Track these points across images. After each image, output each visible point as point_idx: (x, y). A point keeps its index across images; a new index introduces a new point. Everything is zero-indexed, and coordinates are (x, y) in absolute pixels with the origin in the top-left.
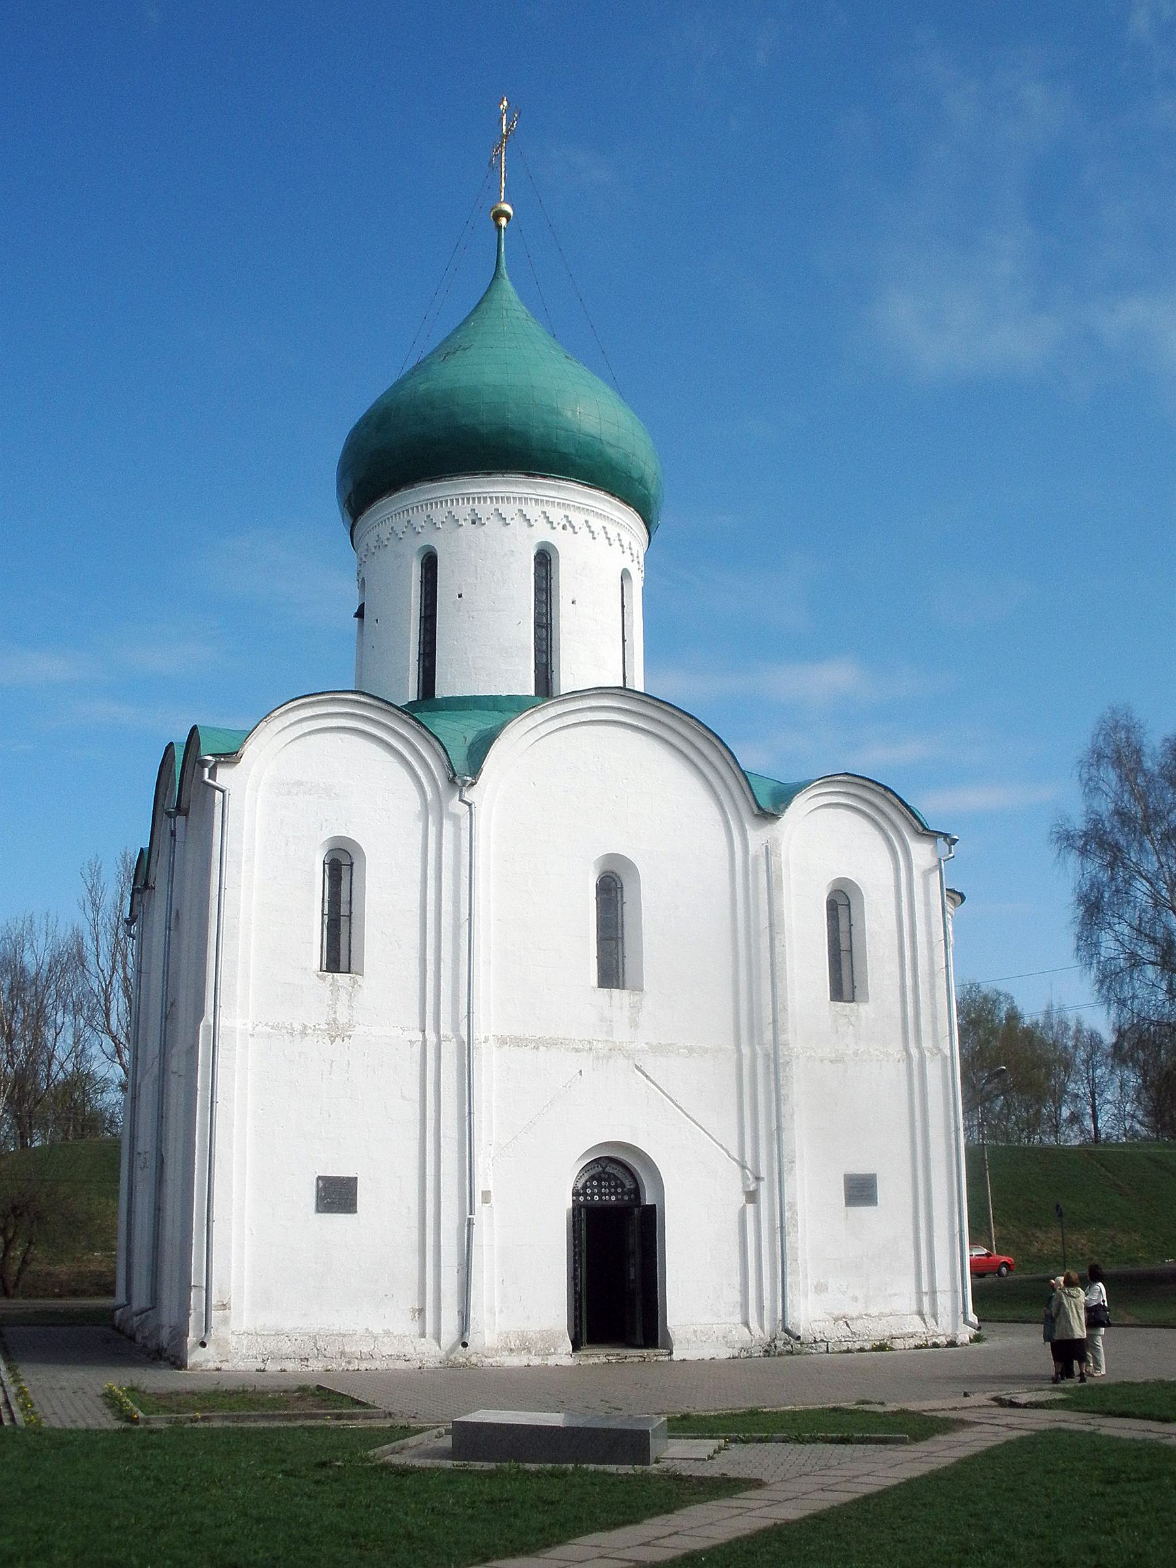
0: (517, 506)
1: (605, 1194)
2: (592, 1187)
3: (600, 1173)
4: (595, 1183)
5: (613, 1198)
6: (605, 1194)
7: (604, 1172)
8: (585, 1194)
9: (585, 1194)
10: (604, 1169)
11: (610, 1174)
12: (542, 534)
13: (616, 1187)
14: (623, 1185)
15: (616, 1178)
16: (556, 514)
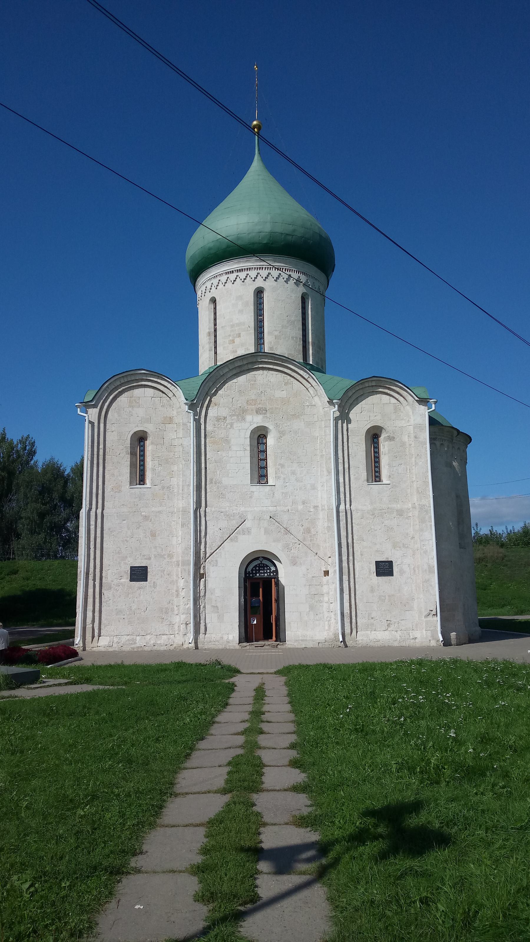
0: (246, 272)
1: (262, 573)
2: (256, 570)
3: (259, 564)
4: (257, 568)
5: (266, 575)
6: (262, 573)
7: (261, 564)
8: (252, 573)
9: (252, 573)
10: (261, 562)
11: (264, 564)
12: (259, 283)
13: (267, 570)
14: (270, 569)
15: (267, 566)
16: (264, 273)
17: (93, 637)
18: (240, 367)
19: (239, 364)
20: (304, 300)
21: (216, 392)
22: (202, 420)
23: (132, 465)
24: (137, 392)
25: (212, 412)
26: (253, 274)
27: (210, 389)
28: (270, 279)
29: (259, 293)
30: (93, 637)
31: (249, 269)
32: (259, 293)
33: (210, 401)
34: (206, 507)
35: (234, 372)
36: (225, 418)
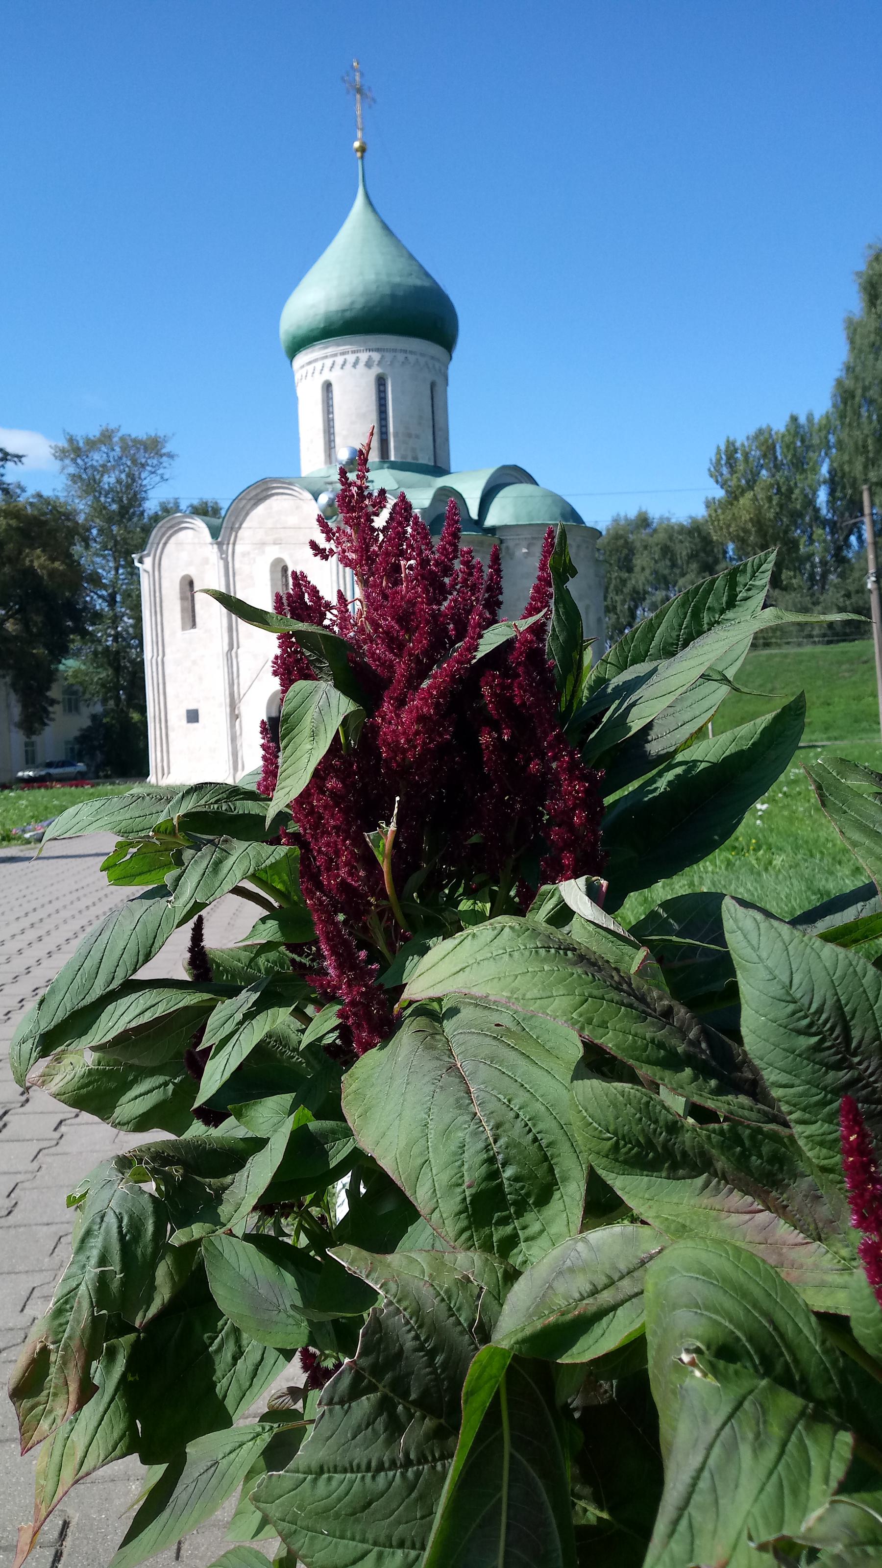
12: (327, 376)
16: (328, 362)
17: (163, 775)
18: (256, 495)
19: (253, 493)
20: (381, 382)
21: (241, 524)
22: (230, 559)
23: (183, 610)
24: (182, 535)
25: (239, 548)
26: (318, 365)
27: (234, 523)
28: (337, 367)
29: (328, 387)
30: (163, 775)
31: (316, 360)
32: (328, 387)
33: (236, 536)
34: (238, 647)
35: (252, 502)
36: (249, 553)
